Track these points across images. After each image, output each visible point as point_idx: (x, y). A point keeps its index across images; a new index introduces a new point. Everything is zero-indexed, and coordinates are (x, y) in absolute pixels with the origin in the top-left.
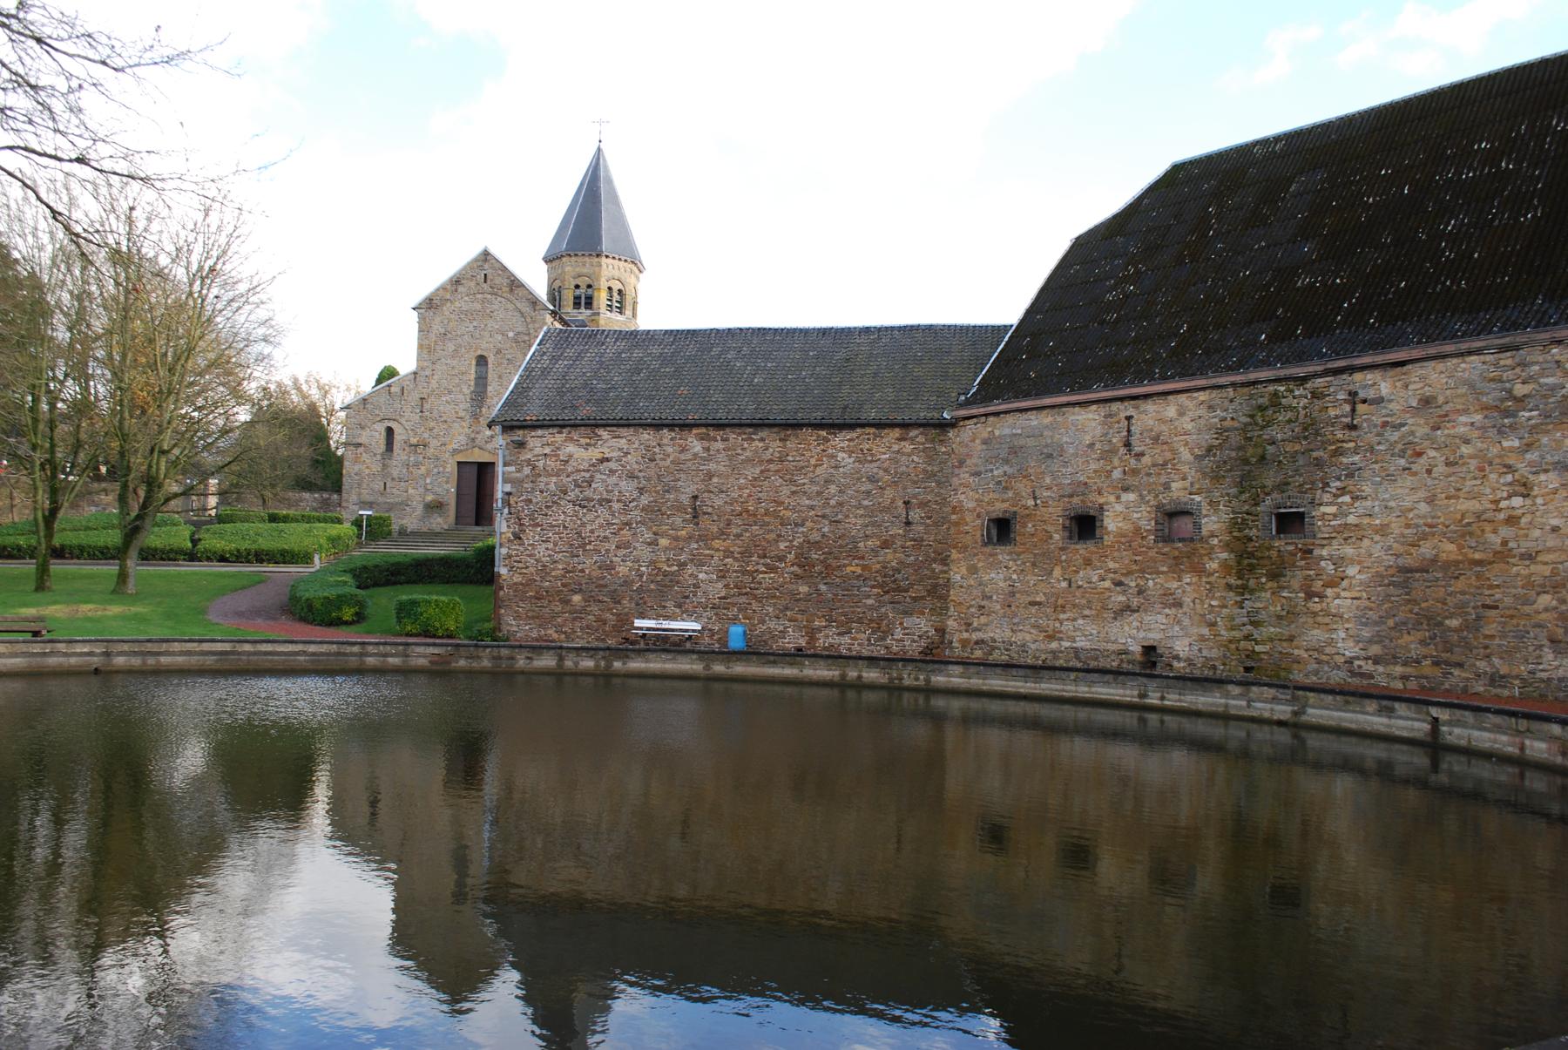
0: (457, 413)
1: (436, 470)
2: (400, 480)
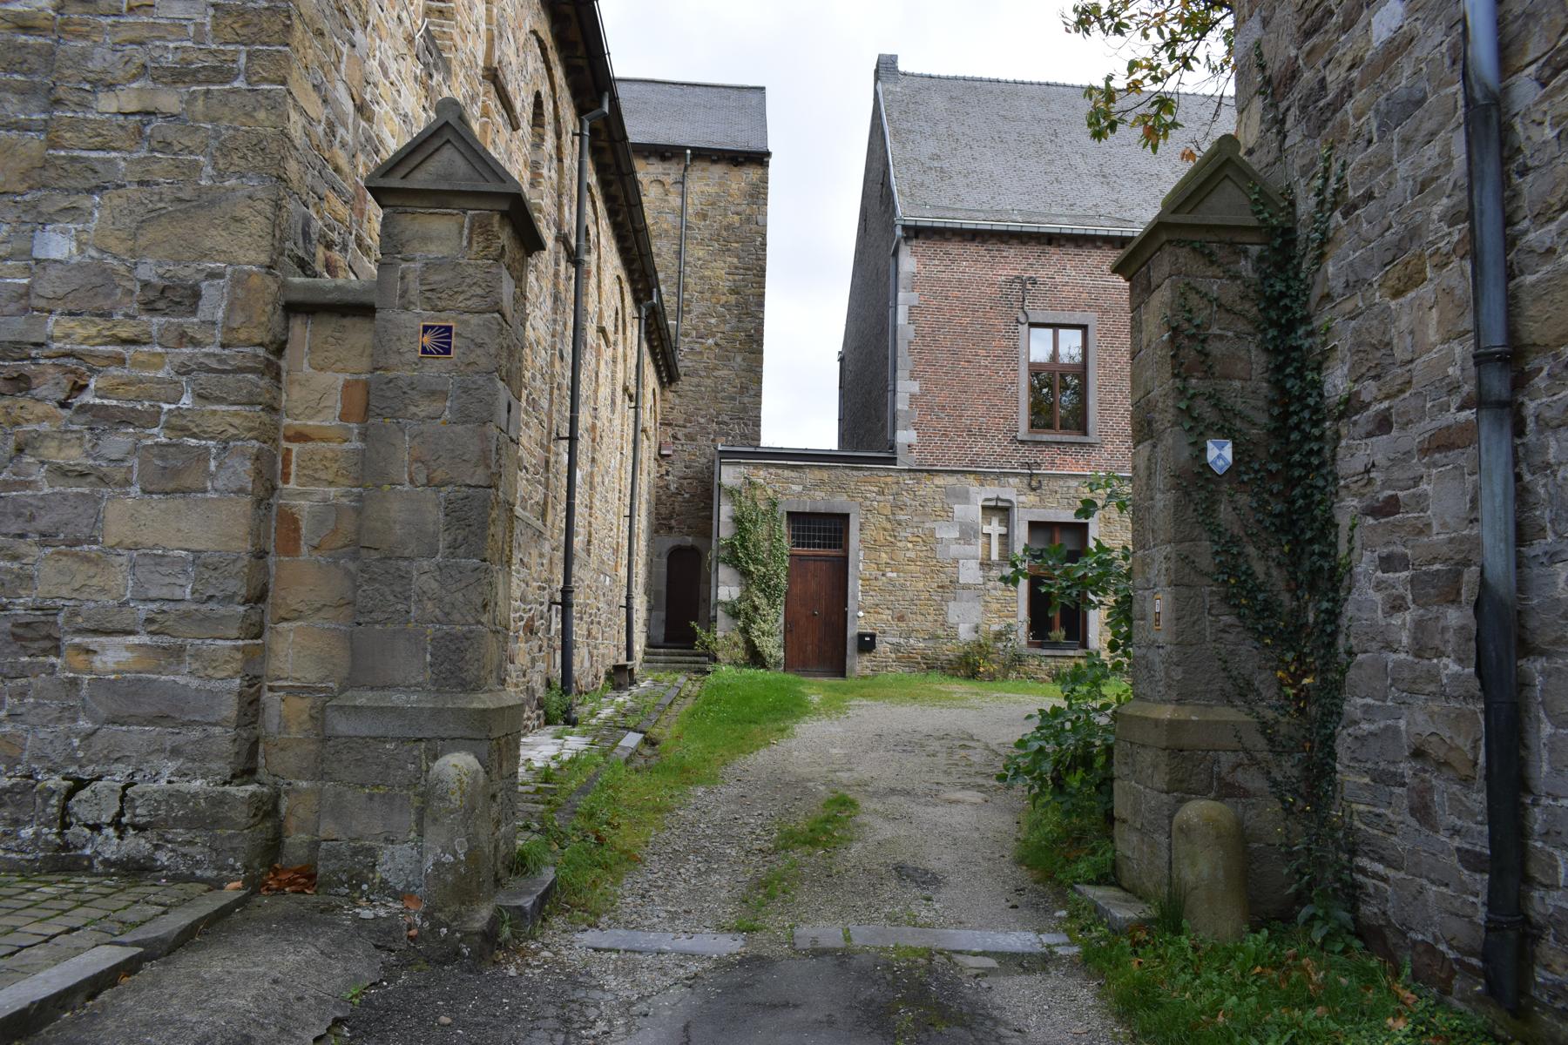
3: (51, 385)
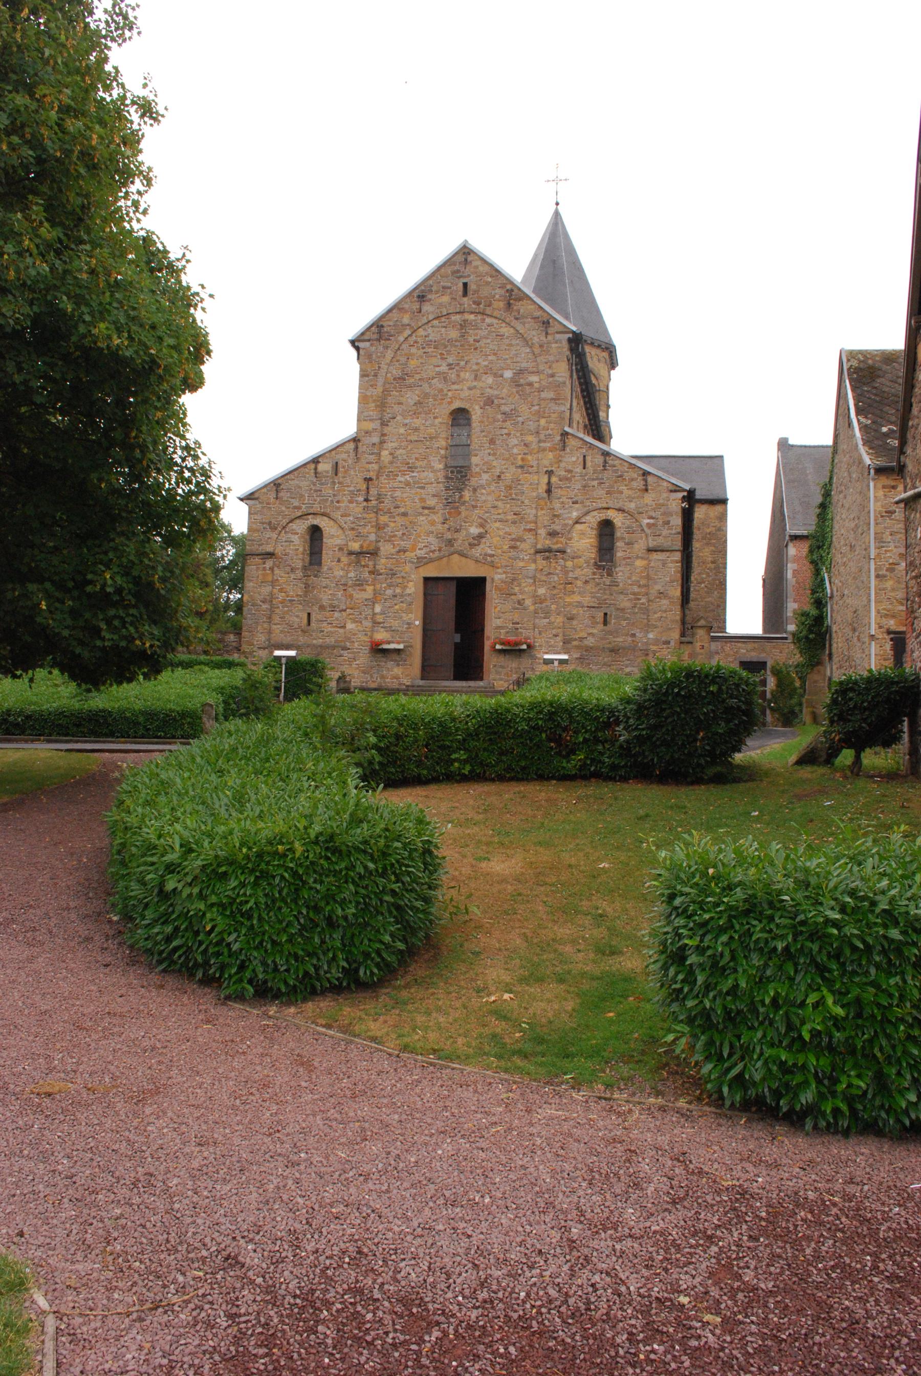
0: (422, 500)
1: (389, 592)
2: (333, 608)
3: (651, 655)
